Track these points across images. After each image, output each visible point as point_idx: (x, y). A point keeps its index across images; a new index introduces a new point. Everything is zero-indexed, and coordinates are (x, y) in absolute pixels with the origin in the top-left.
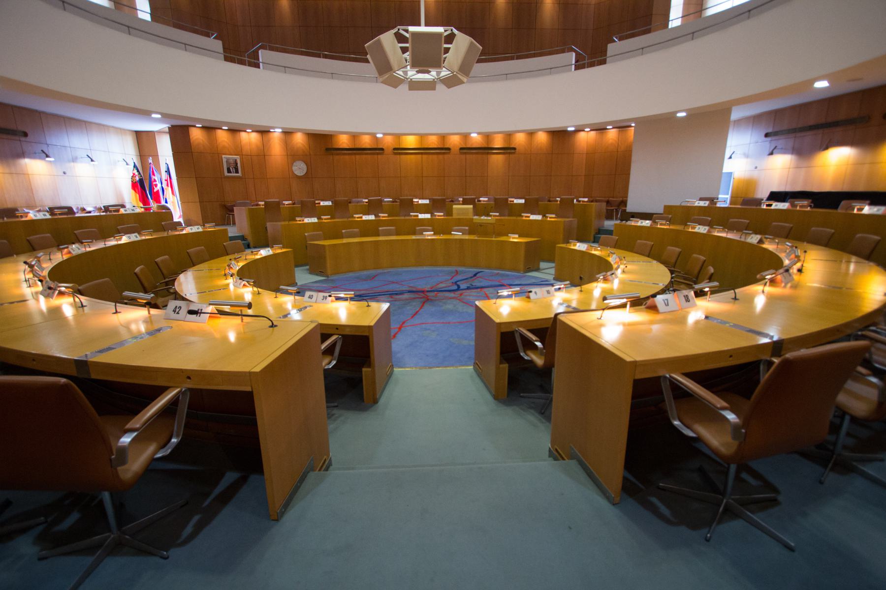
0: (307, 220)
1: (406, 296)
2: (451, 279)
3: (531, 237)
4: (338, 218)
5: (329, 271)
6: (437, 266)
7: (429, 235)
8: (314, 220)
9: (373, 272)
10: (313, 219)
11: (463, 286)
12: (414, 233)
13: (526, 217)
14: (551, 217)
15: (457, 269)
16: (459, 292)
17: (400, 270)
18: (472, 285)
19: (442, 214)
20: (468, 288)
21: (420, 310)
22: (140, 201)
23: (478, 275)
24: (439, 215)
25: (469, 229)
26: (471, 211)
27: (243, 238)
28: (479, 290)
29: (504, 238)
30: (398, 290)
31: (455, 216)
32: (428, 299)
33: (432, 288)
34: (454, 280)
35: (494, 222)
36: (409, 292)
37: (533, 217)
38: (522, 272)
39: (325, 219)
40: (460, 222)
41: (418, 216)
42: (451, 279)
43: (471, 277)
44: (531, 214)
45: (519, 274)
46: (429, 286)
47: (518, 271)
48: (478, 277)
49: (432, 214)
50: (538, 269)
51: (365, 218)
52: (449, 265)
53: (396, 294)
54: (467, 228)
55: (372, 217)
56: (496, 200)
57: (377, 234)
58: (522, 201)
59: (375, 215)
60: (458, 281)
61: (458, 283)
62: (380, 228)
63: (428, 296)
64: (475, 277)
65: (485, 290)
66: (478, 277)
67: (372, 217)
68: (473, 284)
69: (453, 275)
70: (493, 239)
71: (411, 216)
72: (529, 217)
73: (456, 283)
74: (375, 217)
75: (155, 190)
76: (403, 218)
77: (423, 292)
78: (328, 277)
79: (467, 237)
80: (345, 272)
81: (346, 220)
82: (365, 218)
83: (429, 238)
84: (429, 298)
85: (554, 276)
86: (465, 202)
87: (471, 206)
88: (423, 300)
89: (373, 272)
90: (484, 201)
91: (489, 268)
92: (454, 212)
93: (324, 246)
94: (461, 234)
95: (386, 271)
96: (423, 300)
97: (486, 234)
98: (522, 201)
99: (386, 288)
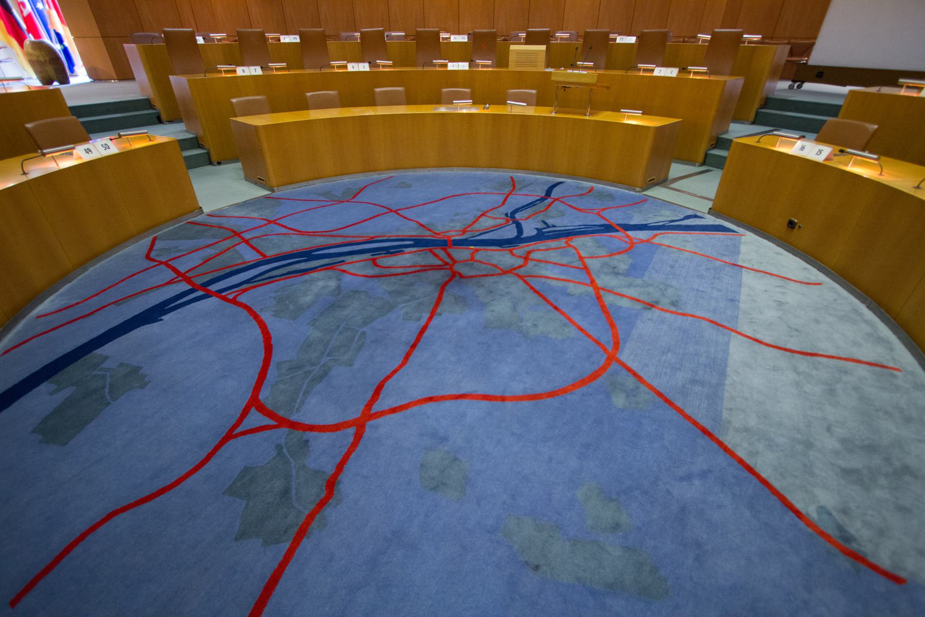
0: (241, 71)
1: (407, 259)
2: (504, 203)
3: (679, 118)
4: (309, 68)
5: (273, 181)
6: (475, 166)
7: (465, 107)
8: (256, 71)
9: (361, 179)
10: (252, 68)
11: (529, 230)
12: (438, 101)
13: (645, 70)
14: (698, 72)
15: (512, 174)
16: (521, 250)
17: (410, 173)
18: (549, 227)
19: (489, 62)
20: (540, 236)
21: (430, 318)
22: (9, 33)
23: (555, 193)
24: (484, 64)
25: (538, 93)
26: (543, 56)
27: (146, 103)
28: (562, 242)
29: (605, 116)
30: (394, 234)
31: (512, 67)
32: (454, 274)
33: (464, 231)
34: (508, 208)
35: (593, 80)
36: (418, 242)
37: (661, 72)
38: (638, 189)
39: (277, 69)
40: (521, 79)
41: (446, 66)
42: (504, 203)
43: (543, 199)
44: (657, 66)
45: (632, 193)
46: (459, 226)
47: (630, 186)
48: (555, 200)
49: (472, 63)
50: (663, 181)
51: (353, 67)
52: (498, 166)
53: (388, 251)
54: (534, 92)
55: (364, 67)
56: (587, 36)
57: (372, 103)
58: (632, 40)
59: (370, 63)
60: (517, 211)
61: (518, 216)
62: (378, 90)
63: (455, 261)
64: (549, 201)
65: (577, 241)
66: (555, 200)
67: (364, 67)
68: (550, 221)
69: (507, 191)
70: (587, 118)
71: (435, 65)
72: (652, 71)
73: (511, 217)
74: (370, 67)
75: (25, 14)
76: (420, 69)
77: (446, 244)
78: (273, 191)
79: (531, 111)
80: (308, 180)
81: (317, 71)
82: (353, 67)
83: (465, 111)
84: (457, 268)
85: (710, 204)
86: (531, 39)
87: (543, 48)
88: (440, 276)
89: (361, 179)
90: (562, 39)
91: (572, 175)
92: (512, 58)
93: (256, 128)
94: (525, 104)
95: (384, 176)
96: (440, 276)
97: (563, 105)
98: (632, 40)
99: (370, 229)
